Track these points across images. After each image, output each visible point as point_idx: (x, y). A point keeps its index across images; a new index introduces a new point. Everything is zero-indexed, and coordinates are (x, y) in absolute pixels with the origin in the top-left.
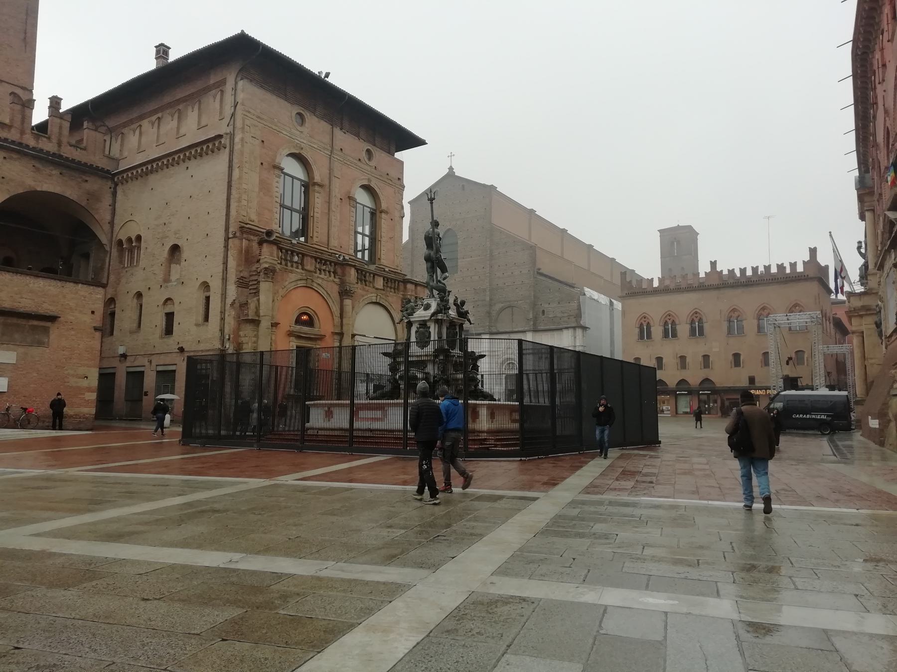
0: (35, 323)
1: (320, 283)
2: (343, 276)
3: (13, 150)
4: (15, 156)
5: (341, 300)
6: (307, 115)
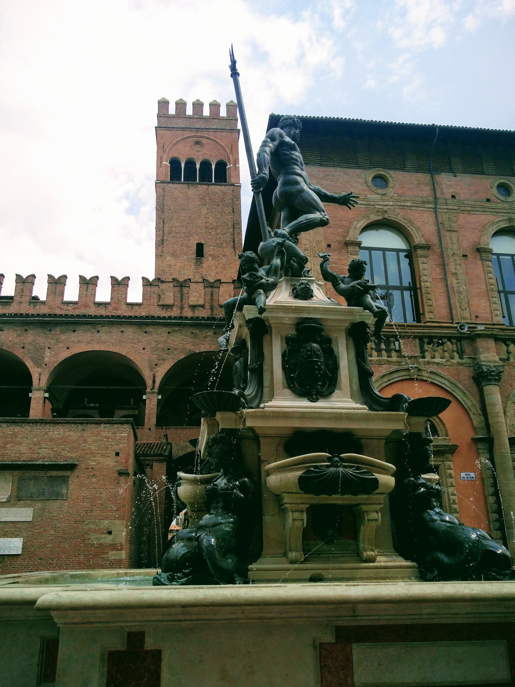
0: (54, 473)
1: (433, 370)
2: (475, 354)
3: (175, 324)
4: (177, 329)
5: (479, 389)
6: (389, 173)
